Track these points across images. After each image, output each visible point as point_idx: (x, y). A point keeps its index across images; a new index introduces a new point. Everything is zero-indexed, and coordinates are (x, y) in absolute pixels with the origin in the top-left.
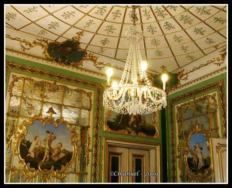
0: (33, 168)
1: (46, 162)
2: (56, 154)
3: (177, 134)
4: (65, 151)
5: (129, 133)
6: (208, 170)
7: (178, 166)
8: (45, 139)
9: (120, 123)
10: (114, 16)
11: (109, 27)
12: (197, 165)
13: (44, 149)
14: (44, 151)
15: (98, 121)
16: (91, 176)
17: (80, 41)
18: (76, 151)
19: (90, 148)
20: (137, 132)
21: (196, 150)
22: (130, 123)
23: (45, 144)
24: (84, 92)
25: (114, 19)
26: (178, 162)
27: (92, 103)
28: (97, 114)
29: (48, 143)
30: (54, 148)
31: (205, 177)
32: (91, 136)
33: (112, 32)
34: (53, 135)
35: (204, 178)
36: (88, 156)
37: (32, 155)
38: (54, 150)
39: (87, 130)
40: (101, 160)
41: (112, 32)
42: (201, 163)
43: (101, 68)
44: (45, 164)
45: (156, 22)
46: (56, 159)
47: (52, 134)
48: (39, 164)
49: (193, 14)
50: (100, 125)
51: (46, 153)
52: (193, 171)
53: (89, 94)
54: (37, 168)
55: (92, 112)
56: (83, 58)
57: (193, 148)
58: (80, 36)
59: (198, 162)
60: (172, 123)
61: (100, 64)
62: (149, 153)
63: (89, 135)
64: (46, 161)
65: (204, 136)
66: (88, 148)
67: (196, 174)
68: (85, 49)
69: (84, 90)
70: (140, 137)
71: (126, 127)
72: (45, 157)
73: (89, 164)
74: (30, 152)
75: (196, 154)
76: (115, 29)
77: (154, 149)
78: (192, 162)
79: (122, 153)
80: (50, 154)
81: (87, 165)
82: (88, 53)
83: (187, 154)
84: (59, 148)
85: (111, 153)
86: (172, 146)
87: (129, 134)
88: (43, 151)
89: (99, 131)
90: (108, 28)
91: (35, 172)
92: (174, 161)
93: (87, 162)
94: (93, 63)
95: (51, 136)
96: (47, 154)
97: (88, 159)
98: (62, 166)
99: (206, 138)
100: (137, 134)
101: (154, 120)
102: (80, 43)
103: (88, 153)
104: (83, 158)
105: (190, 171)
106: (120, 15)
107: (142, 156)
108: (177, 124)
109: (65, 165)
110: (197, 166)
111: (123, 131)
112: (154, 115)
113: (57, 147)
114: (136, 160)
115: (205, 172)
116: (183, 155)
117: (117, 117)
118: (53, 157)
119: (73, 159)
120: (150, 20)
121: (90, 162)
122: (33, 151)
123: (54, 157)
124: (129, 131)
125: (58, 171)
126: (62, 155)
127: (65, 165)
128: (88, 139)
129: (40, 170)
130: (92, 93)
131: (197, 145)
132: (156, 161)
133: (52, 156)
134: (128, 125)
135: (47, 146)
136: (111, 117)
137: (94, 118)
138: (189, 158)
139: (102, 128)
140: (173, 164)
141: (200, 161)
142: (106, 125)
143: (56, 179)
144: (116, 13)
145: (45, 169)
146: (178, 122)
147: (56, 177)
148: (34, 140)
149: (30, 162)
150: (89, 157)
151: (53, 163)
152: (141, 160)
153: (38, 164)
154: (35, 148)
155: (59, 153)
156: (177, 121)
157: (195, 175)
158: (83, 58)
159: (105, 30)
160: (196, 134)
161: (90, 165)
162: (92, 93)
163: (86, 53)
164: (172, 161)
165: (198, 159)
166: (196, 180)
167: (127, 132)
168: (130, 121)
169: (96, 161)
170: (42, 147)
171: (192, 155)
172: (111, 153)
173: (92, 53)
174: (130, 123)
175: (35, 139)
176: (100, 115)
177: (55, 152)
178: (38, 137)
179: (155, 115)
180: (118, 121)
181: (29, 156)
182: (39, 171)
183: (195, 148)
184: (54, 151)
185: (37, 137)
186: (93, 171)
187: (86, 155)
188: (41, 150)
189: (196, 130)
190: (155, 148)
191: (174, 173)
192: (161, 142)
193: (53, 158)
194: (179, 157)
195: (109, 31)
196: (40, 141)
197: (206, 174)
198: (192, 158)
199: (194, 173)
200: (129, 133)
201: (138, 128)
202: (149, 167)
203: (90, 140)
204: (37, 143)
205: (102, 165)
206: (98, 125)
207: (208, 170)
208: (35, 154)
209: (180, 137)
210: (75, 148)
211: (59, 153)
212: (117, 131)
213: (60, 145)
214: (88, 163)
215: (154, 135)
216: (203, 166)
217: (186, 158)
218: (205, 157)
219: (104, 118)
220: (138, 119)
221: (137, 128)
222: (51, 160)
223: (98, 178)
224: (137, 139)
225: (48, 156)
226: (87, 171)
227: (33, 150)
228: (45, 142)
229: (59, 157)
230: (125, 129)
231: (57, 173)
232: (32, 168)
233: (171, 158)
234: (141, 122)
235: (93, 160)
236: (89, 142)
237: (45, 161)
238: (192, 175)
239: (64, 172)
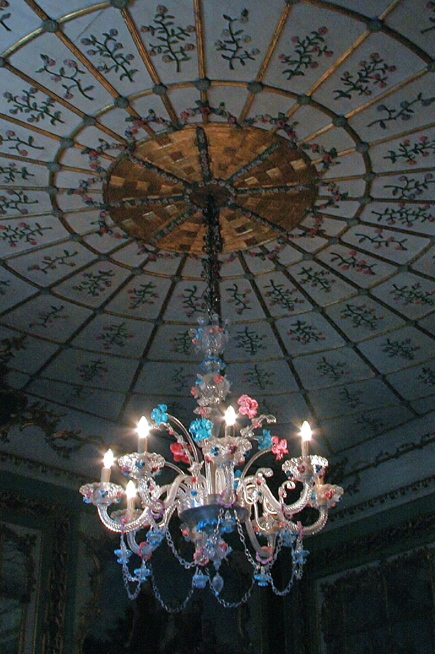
10: (132, 298)
11: (111, 329)
17: (8, 365)
24: (11, 534)
25: (134, 307)
27: (37, 575)
33: (121, 344)
41: (121, 344)
43: (70, 450)
45: (266, 320)
49: (382, 303)
53: (25, 544)
55: (32, 605)
56: (13, 416)
58: (13, 350)
61: (66, 439)
68: (23, 390)
69: (11, 526)
76: (131, 336)
82: (32, 400)
90: (109, 332)
94: (44, 434)
102: (6, 371)
106: (152, 299)
120: (246, 316)
130: (35, 537)
144: (140, 292)
158: (13, 416)
159: (99, 338)
162: (35, 537)
163: (24, 401)
173: (43, 402)
195: (109, 339)
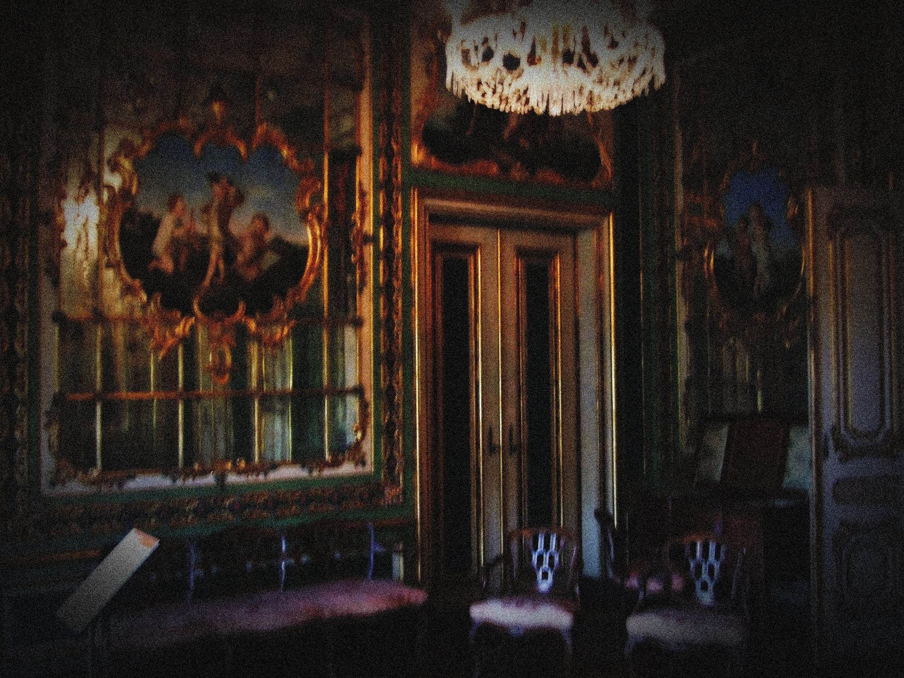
4: (279, 244)
13: (206, 240)
23: (208, 223)
40: (407, 270)
51: (213, 257)
63: (360, 184)
66: (361, 230)
80: (229, 255)
83: (713, 247)
84: (257, 237)
100: (533, 173)
111: (480, 166)
122: (166, 249)
126: (270, 259)
135: (216, 231)
139: (406, 154)
161: (369, 291)
175: (171, 206)
210: (314, 234)
222: (233, 276)
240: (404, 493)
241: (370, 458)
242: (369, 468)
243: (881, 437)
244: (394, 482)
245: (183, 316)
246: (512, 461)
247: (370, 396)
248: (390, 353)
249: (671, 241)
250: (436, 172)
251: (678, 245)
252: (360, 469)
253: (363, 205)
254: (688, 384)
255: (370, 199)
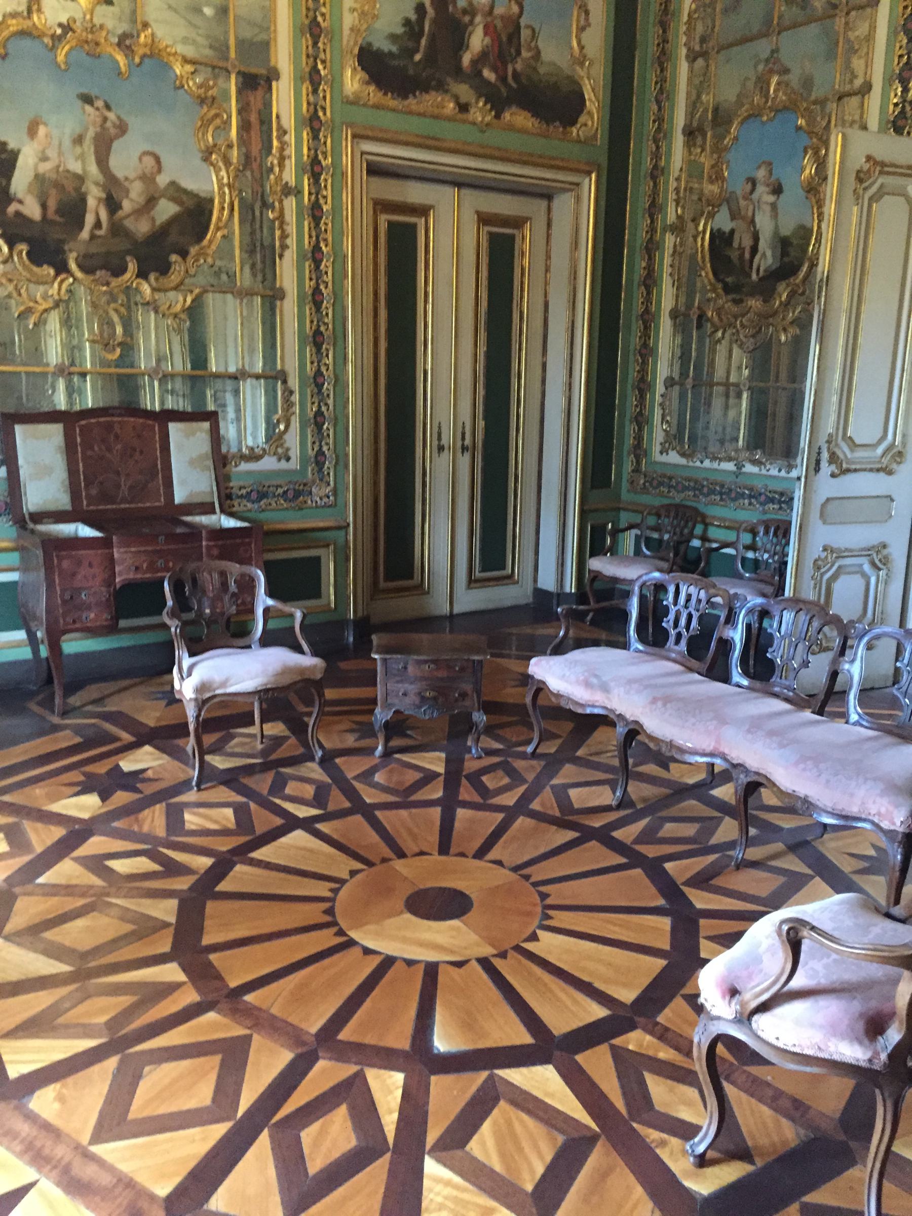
0: (45, 266)
1: (100, 240)
2: (136, 206)
3: (680, 119)
4: (176, 192)
5: (463, 108)
6: (788, 285)
7: (667, 270)
8: (78, 131)
9: (418, 57)
12: (747, 265)
13: (80, 179)
14: (83, 190)
15: (315, 44)
16: (299, 306)
18: (227, 190)
19: (289, 176)
20: (498, 104)
21: (755, 196)
22: (466, 59)
23: (82, 157)
26: (671, 251)
28: (308, 9)
29: (92, 149)
30: (127, 179)
31: (775, 313)
32: (289, 122)
34: (111, 116)
35: (771, 320)
36: (281, 217)
37: (32, 210)
38: (126, 184)
39: (270, 88)
40: (339, 234)
42: (764, 254)
44: (93, 249)
46: (142, 228)
47: (108, 107)
48: (71, 251)
50: (328, 64)
51: (91, 202)
52: (727, 289)
54: (62, 268)
57: (739, 187)
59: (754, 250)
60: (661, 64)
62: (549, 210)
63: (278, 117)
64: (99, 237)
65: (799, 128)
66: (279, 178)
67: (737, 302)
70: (511, 128)
71: (449, 80)
72: (90, 219)
73: (287, 254)
74: (20, 195)
75: (750, 214)
77: (571, 190)
78: (728, 253)
79: (431, 207)
80: (112, 204)
81: (281, 256)
83: (711, 215)
84: (148, 179)
85: (381, 206)
86: (654, 177)
87: (460, 116)
88: (78, 189)
89: (324, 98)
91: (56, 285)
92: (652, 248)
93: (277, 244)
95: (105, 119)
96: (98, 206)
97: (283, 231)
98: (174, 258)
99: (805, 140)
100: (498, 116)
101: (582, 48)
103: (281, 202)
104: (261, 222)
105: (714, 290)
107: (518, 223)
108: (683, 68)
109: (184, 254)
110: (747, 269)
111: (430, 100)
112: (582, 22)
113: (140, 172)
114: (492, 237)
115: (775, 296)
116: (695, 220)
117: (404, 25)
118: (128, 216)
119: (218, 229)
121: (292, 242)
122: (29, 191)
123: (132, 217)
124: (463, 100)
125: (157, 279)
126: (166, 210)
127: (184, 254)
128: (275, 134)
129: (79, 274)
131: (761, 174)
132: (576, 244)
133: (120, 213)
134: (457, 71)
135: (93, 169)
136: (378, 25)
137: (299, 31)
138: (719, 230)
139: (336, 82)
140: (650, 258)
141: (762, 245)
142: (354, 70)
143: (153, 315)
145: (98, 273)
146: (692, 57)
147: (151, 308)
148: (25, 137)
149: (23, 239)
150: (287, 218)
151: (129, 247)
152: (512, 238)
153: (66, 248)
154: (39, 178)
155: (151, 202)
156: (684, 51)
157: (735, 309)
160: (765, 118)
161: (290, 256)
164: (647, 248)
165: (756, 238)
166: (735, 327)
167: (452, 105)
168: (468, 47)
169: (317, 237)
170: (68, 171)
171: (733, 218)
172: (381, 206)
174: (466, 59)
175: (32, 131)
176: (323, 15)
177: (133, 194)
178: (46, 124)
179: (587, 19)
180: (411, 44)
181: (18, 214)
182: (75, 279)
183: (749, 186)
184: (127, 191)
185: (38, 124)
186: (307, 281)
187: (273, 209)
188: (69, 186)
189: (767, 102)
190: (578, 184)
191: (648, 300)
192: (604, 161)
193: (129, 224)
194: (678, 228)
196: (56, 142)
197: (777, 303)
198: (732, 232)
199: (730, 297)
200: (463, 108)
201: (503, 90)
202: (547, 270)
203: (286, 138)
204: (43, 152)
205: (345, 257)
206: (320, 66)
207: (788, 285)
208: (44, 206)
209: (690, 133)
210: (220, 180)
211: (151, 202)
212: (405, 97)
213: (149, 161)
214: (284, 247)
215: (573, 123)
216: (774, 267)
217: (704, 232)
218: (787, 230)
219: (346, 32)
220: (504, 39)
221: (498, 84)
222: (117, 229)
223: (330, 315)
224: (495, 138)
225: (104, 215)
226: (281, 281)
227: (30, 184)
228: (78, 150)
229: (153, 220)
230: (441, 87)
231: (154, 289)
232: (39, 265)
233: (642, 235)
234: (519, 53)
235: (307, 236)
236: (282, 149)
237: (93, 237)
238: (723, 307)
239: (182, 283)
240: (335, 491)
241: (295, 453)
242: (294, 464)
243: (880, 450)
244: (323, 479)
245: (57, 274)
246: (464, 461)
247: (294, 382)
248: (317, 333)
249: (662, 209)
250: (377, 107)
251: (671, 217)
252: (283, 465)
253: (283, 146)
254: (670, 383)
255: (291, 138)
